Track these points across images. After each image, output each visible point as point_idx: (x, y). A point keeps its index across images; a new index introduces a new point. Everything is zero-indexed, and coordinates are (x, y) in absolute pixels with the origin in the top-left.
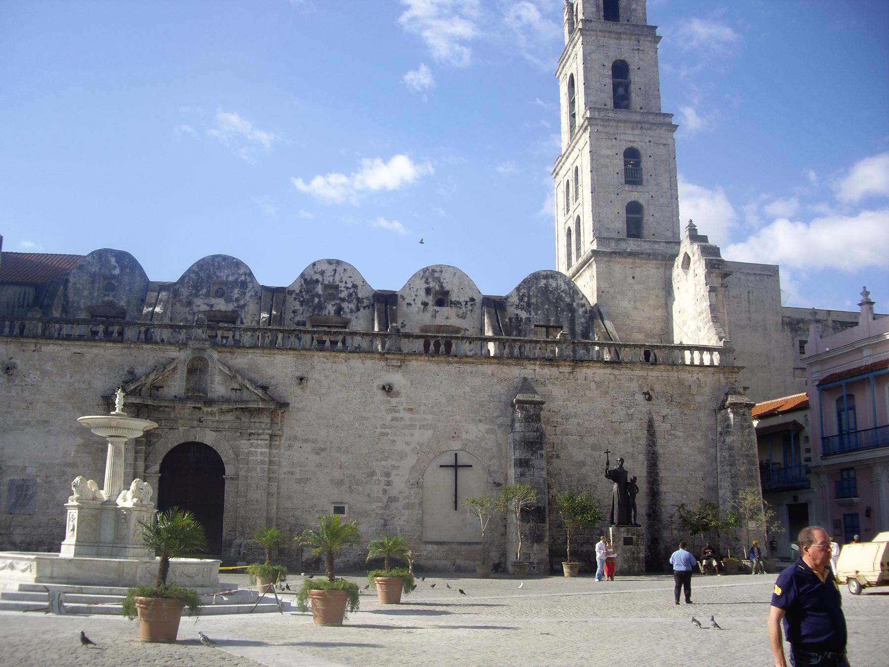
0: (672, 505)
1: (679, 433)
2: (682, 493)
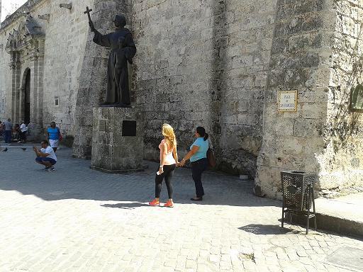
0: (241, 76)
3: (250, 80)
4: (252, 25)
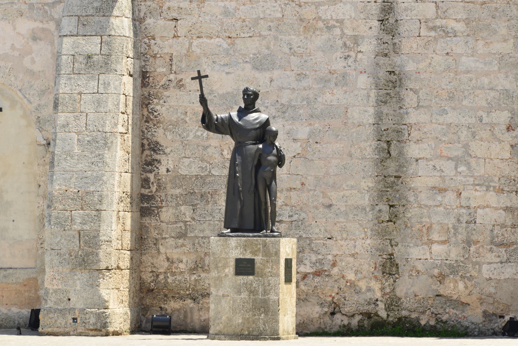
1: (452, 24)
2: (457, 161)
3: (450, 197)
4: (451, 117)
